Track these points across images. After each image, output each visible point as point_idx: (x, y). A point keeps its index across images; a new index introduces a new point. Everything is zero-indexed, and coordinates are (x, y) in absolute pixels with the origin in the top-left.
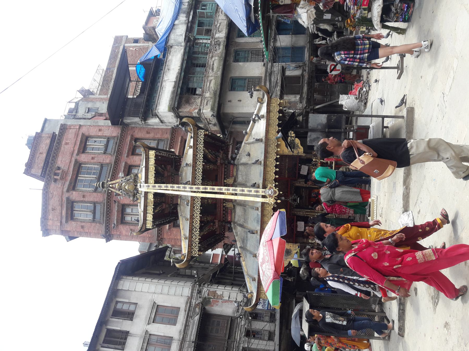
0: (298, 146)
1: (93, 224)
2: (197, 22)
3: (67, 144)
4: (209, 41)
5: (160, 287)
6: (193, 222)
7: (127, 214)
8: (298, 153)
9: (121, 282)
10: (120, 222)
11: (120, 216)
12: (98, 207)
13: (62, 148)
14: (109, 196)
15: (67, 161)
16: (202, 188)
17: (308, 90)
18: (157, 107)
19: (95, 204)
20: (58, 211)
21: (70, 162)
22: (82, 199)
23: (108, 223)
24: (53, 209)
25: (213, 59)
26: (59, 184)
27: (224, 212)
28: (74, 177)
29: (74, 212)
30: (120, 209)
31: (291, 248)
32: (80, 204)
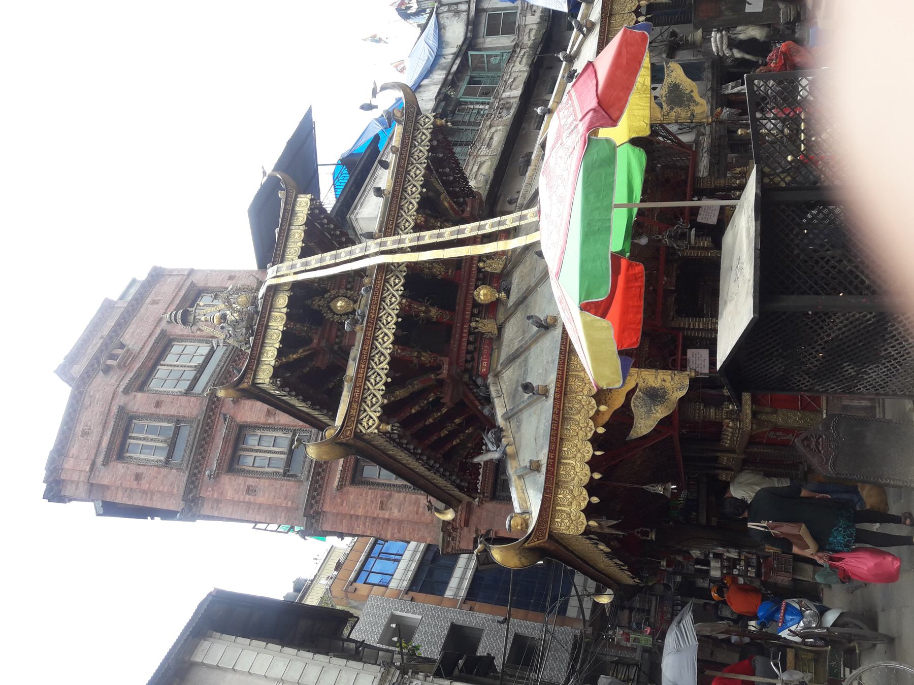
0: (691, 99)
1: (164, 471)
2: (467, 79)
3: (154, 302)
4: (487, 107)
5: (298, 666)
6: (375, 338)
7: (245, 450)
8: (693, 115)
9: (205, 644)
10: (225, 467)
11: (229, 452)
12: (186, 432)
13: (142, 311)
14: (214, 403)
15: (145, 334)
16: (409, 239)
17: (711, 164)
18: (355, 209)
19: (179, 422)
20: (94, 437)
21: (150, 336)
22: (153, 410)
23: (196, 468)
24: (85, 434)
25: (493, 130)
26: (113, 378)
27: (471, 347)
28: (152, 362)
29: (130, 441)
30: (233, 436)
31: (668, 385)
32: (147, 423)
